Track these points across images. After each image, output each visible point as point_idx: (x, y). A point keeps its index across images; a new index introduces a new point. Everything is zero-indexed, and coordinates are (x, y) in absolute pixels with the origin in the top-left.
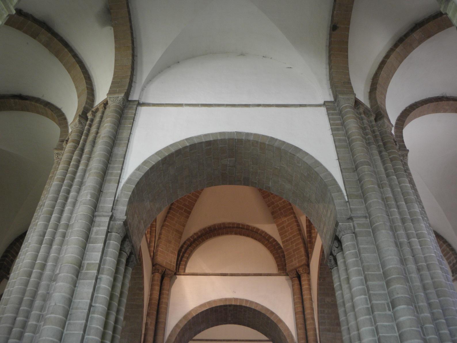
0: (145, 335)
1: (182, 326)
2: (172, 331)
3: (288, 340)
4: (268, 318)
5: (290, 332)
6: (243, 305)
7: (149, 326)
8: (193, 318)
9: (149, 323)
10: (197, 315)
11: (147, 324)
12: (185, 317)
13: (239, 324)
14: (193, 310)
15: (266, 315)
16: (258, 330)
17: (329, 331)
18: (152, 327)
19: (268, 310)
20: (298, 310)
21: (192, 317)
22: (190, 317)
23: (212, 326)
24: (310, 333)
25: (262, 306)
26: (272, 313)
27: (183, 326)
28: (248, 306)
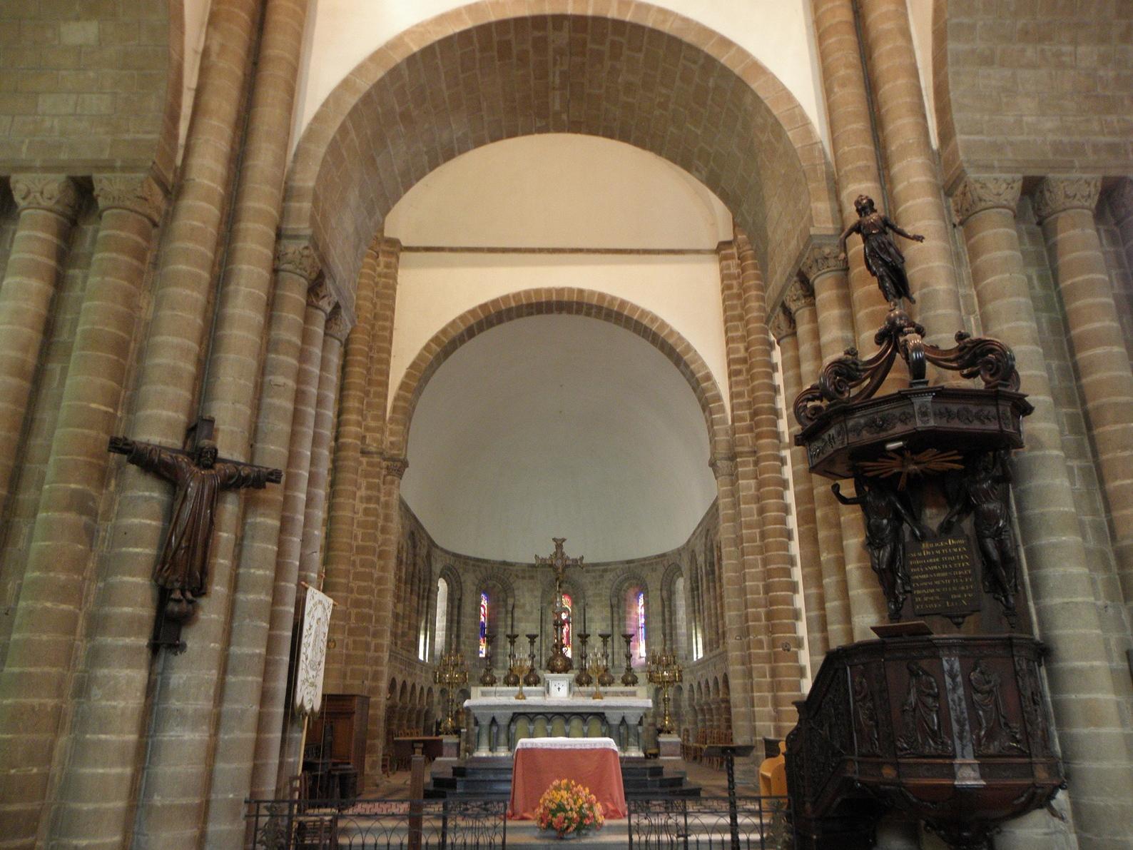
0: (199, 92)
1: (365, 85)
2: (325, 104)
3: (789, 134)
4: (710, 63)
5: (799, 106)
6: (610, 16)
7: (214, 58)
8: (411, 59)
9: (215, 48)
10: (428, 51)
11: (206, 54)
12: (376, 57)
13: (592, 131)
14: (408, 33)
15: (698, 51)
16: (658, 149)
17: (987, 60)
18: (230, 69)
19: (709, 33)
20: (837, 20)
21: (406, 55)
22: (398, 57)
23: (495, 139)
24: (893, 91)
25: (686, 20)
26: (726, 43)
27: (368, 87)
28: (628, 17)
